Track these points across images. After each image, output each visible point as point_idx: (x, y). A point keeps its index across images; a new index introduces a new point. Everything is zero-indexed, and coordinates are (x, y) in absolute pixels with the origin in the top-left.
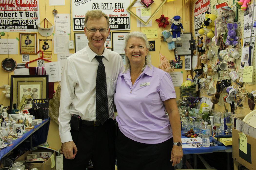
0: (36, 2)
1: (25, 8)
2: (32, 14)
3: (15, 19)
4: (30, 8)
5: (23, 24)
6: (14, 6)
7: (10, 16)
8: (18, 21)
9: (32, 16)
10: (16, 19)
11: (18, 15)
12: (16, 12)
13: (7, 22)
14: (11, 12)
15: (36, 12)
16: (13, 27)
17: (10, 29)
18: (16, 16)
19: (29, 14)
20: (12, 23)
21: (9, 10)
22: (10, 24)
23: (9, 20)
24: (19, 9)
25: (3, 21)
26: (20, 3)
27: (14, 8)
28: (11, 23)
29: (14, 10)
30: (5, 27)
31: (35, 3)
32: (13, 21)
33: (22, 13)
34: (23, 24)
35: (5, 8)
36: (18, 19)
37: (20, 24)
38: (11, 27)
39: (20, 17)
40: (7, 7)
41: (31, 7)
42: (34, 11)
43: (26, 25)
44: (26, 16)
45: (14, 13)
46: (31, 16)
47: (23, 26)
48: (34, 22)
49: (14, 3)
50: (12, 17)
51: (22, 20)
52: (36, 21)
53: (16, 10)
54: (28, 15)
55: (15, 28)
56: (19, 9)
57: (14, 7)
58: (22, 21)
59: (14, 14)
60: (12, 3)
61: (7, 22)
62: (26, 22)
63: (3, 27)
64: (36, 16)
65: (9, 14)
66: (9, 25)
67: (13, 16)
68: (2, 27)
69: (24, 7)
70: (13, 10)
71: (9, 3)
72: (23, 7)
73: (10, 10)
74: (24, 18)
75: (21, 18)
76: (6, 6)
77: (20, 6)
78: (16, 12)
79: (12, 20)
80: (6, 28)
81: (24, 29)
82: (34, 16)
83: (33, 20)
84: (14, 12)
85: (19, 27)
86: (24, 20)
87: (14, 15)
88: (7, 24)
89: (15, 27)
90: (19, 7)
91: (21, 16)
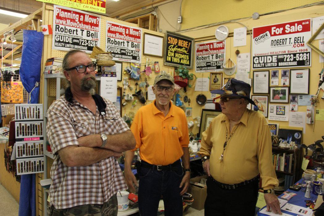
0: (98, 21)
3: (75, 37)
4: (91, 28)
5: (83, 44)
6: (77, 22)
7: (70, 32)
8: (78, 39)
10: (76, 38)
11: (79, 32)
12: (77, 29)
13: (67, 39)
14: (73, 29)
16: (73, 45)
17: (70, 47)
19: (90, 34)
20: (72, 41)
21: (70, 26)
22: (70, 42)
23: (69, 37)
24: (80, 26)
25: (63, 37)
26: (82, 20)
27: (75, 24)
28: (71, 41)
29: (75, 26)
31: (97, 22)
32: (73, 39)
33: (83, 32)
34: (83, 44)
36: (79, 38)
37: (80, 44)
38: (70, 45)
39: (81, 36)
41: (93, 27)
42: (95, 31)
44: (87, 36)
45: (76, 30)
47: (83, 46)
48: (94, 44)
49: (77, 19)
51: (82, 39)
53: (78, 27)
54: (88, 35)
55: (75, 48)
56: (80, 26)
57: (76, 23)
58: (82, 41)
59: (75, 30)
61: (67, 39)
62: (86, 43)
63: (62, 44)
64: (97, 38)
66: (68, 43)
67: (73, 34)
68: (61, 45)
70: (74, 27)
71: (71, 18)
72: (85, 25)
73: (71, 26)
74: (85, 37)
75: (82, 36)
77: (82, 23)
78: (77, 29)
80: (65, 46)
82: (95, 37)
83: (93, 41)
84: (75, 29)
86: (85, 40)
88: (67, 41)
89: (75, 46)
90: (81, 23)
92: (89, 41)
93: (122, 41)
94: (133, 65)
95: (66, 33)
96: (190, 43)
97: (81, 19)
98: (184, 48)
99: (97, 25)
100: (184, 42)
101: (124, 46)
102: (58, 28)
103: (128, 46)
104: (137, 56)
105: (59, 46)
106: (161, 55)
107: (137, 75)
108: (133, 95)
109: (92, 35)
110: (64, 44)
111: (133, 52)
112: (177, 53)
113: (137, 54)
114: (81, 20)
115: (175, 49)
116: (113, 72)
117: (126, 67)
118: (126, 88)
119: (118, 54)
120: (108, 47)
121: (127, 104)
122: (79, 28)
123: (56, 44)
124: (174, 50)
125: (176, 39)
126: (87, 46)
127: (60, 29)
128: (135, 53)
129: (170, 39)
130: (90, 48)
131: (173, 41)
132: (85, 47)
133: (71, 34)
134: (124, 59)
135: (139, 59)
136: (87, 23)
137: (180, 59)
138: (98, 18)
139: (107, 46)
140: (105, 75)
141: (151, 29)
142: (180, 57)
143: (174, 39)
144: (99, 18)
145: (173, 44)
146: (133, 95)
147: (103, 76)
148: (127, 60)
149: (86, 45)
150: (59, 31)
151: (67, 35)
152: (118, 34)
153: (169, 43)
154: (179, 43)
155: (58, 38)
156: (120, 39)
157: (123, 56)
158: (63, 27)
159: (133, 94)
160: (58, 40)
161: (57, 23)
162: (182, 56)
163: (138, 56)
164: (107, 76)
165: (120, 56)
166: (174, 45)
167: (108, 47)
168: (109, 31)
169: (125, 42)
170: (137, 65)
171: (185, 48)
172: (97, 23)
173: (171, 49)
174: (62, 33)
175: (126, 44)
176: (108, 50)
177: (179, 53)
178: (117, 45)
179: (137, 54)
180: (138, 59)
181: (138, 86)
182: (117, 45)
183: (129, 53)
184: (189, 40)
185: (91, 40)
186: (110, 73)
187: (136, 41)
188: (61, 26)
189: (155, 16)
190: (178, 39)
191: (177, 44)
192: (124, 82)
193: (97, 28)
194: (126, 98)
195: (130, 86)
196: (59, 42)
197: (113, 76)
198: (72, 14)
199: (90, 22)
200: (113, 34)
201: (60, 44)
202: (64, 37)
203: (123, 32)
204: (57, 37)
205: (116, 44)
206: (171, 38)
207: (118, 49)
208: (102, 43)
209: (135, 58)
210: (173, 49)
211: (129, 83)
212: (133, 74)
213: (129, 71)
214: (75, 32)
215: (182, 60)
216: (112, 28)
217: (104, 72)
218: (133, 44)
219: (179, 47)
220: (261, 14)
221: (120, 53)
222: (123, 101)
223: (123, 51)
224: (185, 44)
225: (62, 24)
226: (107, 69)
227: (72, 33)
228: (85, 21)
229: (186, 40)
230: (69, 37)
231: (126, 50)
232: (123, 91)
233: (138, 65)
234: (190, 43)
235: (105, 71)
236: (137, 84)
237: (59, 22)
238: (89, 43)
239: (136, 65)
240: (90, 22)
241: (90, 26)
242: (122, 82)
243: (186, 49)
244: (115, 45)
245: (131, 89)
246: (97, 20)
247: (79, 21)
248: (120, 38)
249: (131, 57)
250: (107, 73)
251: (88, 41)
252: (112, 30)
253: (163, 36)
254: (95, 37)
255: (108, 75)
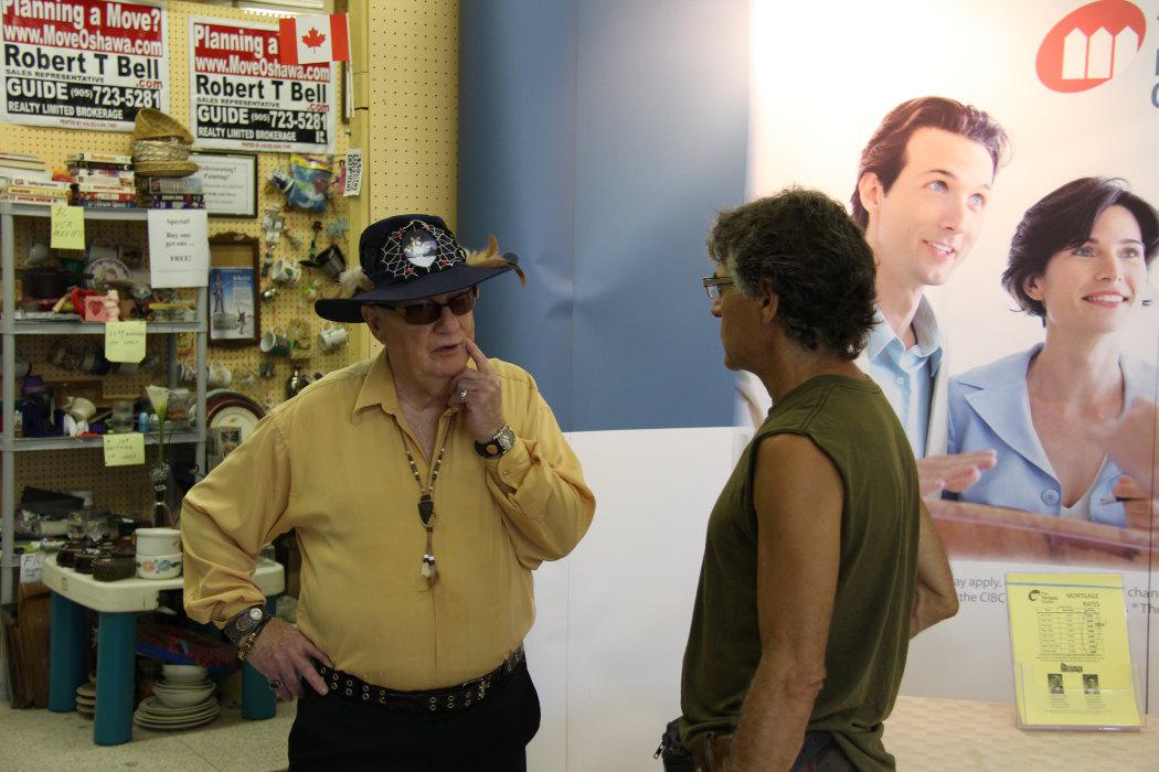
1: (118, 43)
2: (141, 65)
3: (77, 81)
4: (133, 45)
5: (106, 102)
7: (59, 66)
8: (89, 87)
9: (142, 76)
10: (81, 82)
11: (92, 64)
12: (81, 55)
15: (156, 61)
16: (71, 108)
17: (59, 115)
18: (83, 71)
19: (132, 66)
20: (68, 94)
21: (56, 45)
22: (60, 97)
23: (55, 83)
24: (92, 42)
26: (98, 22)
28: (63, 94)
29: (76, 46)
30: (41, 108)
31: (152, 25)
32: (70, 86)
33: (105, 61)
34: (106, 102)
35: (42, 35)
37: (97, 102)
38: (61, 107)
39: (97, 75)
40: (49, 30)
41: (138, 42)
42: (150, 55)
43: (290, 127)
44: (121, 74)
45: (77, 56)
46: (139, 73)
47: (107, 107)
48: (148, 98)
49: (77, 19)
50: (65, 72)
52: (156, 96)
53: (84, 46)
54: (125, 70)
55: (78, 115)
57: (75, 34)
60: (70, 20)
62: (117, 96)
63: (32, 104)
64: (157, 77)
65: (55, 57)
66: (54, 101)
67: (70, 69)
68: (29, 107)
69: (111, 36)
70: (71, 46)
71: (58, 19)
72: (108, 38)
73: (60, 44)
76: (46, 27)
77: (98, 32)
78: (81, 55)
79: (68, 84)
80: (45, 112)
81: (110, 119)
82: (149, 76)
83: (143, 90)
84: (75, 53)
85: (94, 111)
86: (111, 87)
87: (75, 64)
88: (47, 96)
89: (78, 108)
90: (95, 34)
91: (102, 72)
92: (128, 92)
93: (255, 81)
94: (302, 162)
95: (42, 70)
97: (92, 18)
99: (153, 36)
101: (262, 97)
102: (15, 56)
103: (277, 97)
104: (318, 128)
105: (23, 112)
107: (312, 195)
108: (303, 263)
109: (136, 71)
110: (38, 106)
111: (300, 115)
113: (317, 121)
114: (93, 22)
116: (192, 192)
117: (271, 168)
118: (276, 240)
119: (238, 126)
120: (199, 106)
121: (277, 294)
122: (88, 49)
123: (11, 107)
126: (122, 106)
127: (20, 58)
128: (307, 120)
130: (130, 114)
132: (115, 111)
133: (61, 73)
134: (263, 142)
135: (325, 137)
136: (118, 32)
138: (154, 12)
139: (195, 103)
140: (163, 204)
144: (159, 9)
146: (303, 263)
147: (156, 208)
148: (276, 147)
149: (117, 104)
150: (18, 64)
151: (47, 74)
152: (237, 57)
155: (16, 87)
156: (246, 74)
157: (261, 134)
158: (33, 49)
159: (306, 258)
160: (18, 93)
161: (8, 38)
163: (321, 129)
164: (169, 205)
165: (249, 133)
167: (199, 106)
168: (202, 51)
169: (267, 83)
170: (318, 162)
172: (156, 29)
174: (27, 69)
175: (269, 89)
176: (200, 114)
178: (235, 97)
179: (317, 121)
180: (322, 141)
181: (323, 235)
182: (235, 97)
183: (282, 121)
185: (134, 85)
186: (181, 198)
187: (310, 77)
188: (23, 48)
192: (265, 220)
193: (154, 44)
194: (274, 274)
195: (290, 234)
196: (21, 98)
197: (193, 208)
198: (58, 5)
199: (127, 26)
200: (216, 60)
201: (24, 107)
202: (39, 83)
203: (258, 49)
204: (14, 84)
205: (231, 94)
207: (238, 108)
208: (179, 99)
209: (306, 136)
211: (288, 222)
212: (298, 190)
213: (283, 184)
214: (255, 91)
216: (211, 39)
217: (160, 196)
218: (297, 88)
221: (247, 122)
222: (263, 285)
223: (257, 117)
225: (28, 42)
226: (167, 186)
227: (247, 93)
228: (109, 24)
230: (55, 83)
231: (271, 113)
232: (263, 250)
233: (324, 159)
235: (162, 191)
236: (317, 227)
237: (16, 36)
238: (128, 96)
239: (311, 160)
240: (127, 26)
241: (128, 41)
242: (259, 220)
244: (227, 97)
245: (294, 245)
246: (153, 18)
247: (87, 25)
248: (243, 72)
249: (293, 136)
250: (172, 198)
251: (123, 90)
252: (213, 47)
254: (149, 76)
255: (174, 204)
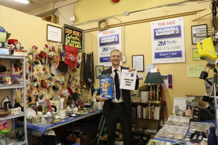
96: (81, 33)
98: (77, 37)
100: (77, 32)
106: (60, 41)
112: (72, 40)
115: (71, 37)
124: (70, 38)
125: (71, 30)
129: (67, 30)
131: (69, 31)
137: (75, 45)
141: (53, 22)
142: (74, 43)
143: (69, 30)
145: (69, 33)
153: (66, 32)
154: (74, 33)
162: (76, 42)
166: (70, 34)
171: (78, 36)
173: (67, 37)
177: (73, 40)
184: (81, 31)
189: (56, 16)
190: (73, 30)
191: (72, 34)
206: (68, 29)
210: (69, 37)
215: (76, 45)
219: (73, 36)
220: (130, 12)
224: (78, 34)
229: (78, 31)
234: (81, 33)
243: (79, 37)
253: (62, 27)
